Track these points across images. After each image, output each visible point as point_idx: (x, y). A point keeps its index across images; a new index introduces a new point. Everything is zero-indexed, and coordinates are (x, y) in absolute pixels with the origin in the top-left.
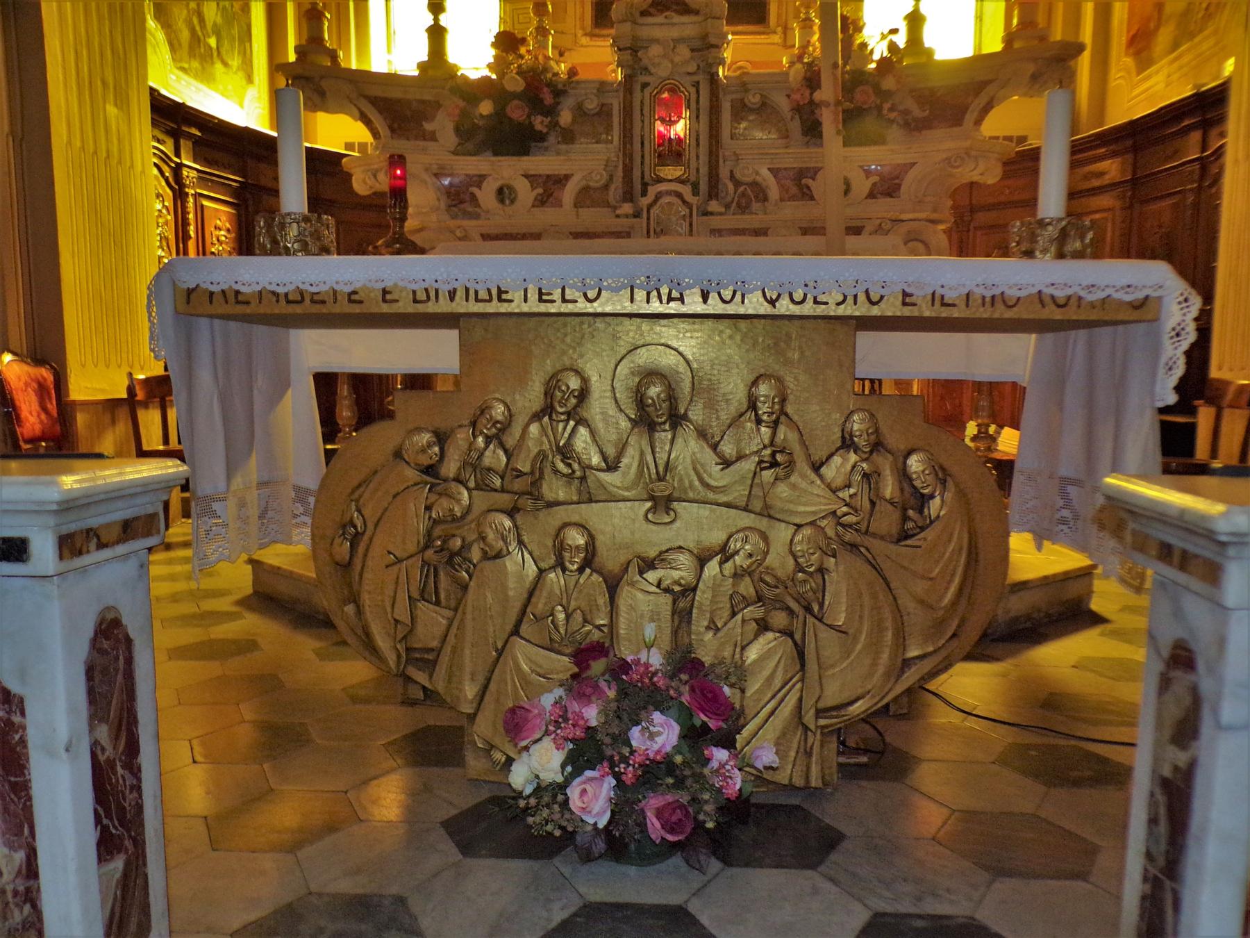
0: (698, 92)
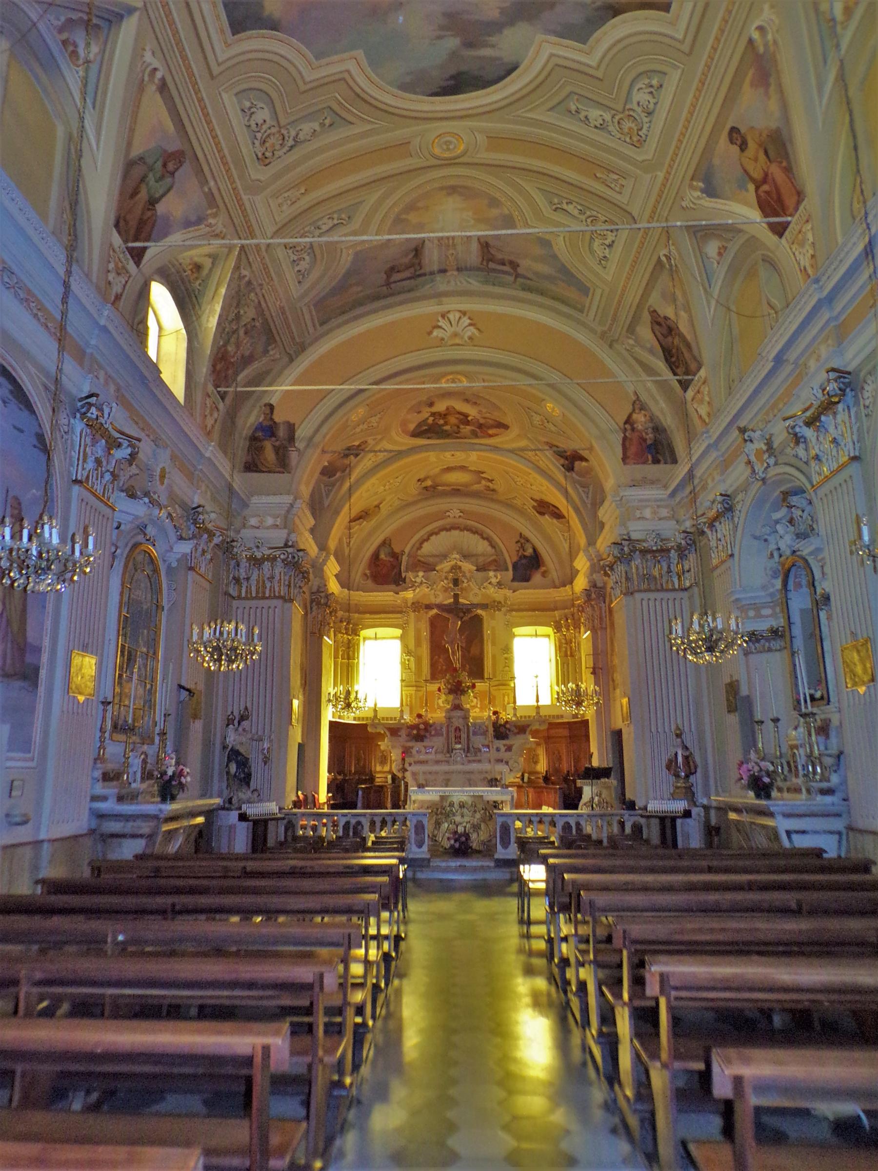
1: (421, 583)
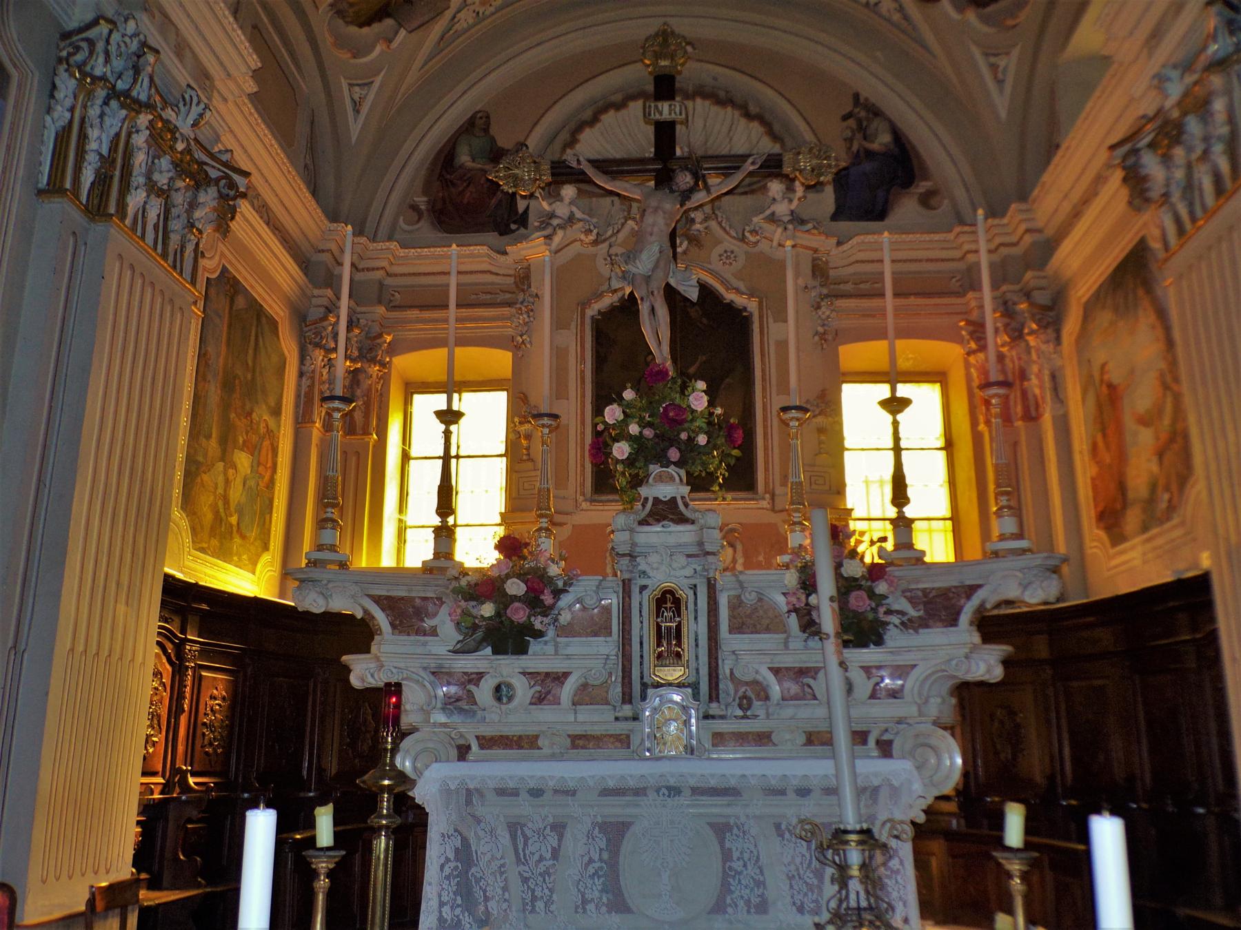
0: (695, 594)
1: (571, 219)
